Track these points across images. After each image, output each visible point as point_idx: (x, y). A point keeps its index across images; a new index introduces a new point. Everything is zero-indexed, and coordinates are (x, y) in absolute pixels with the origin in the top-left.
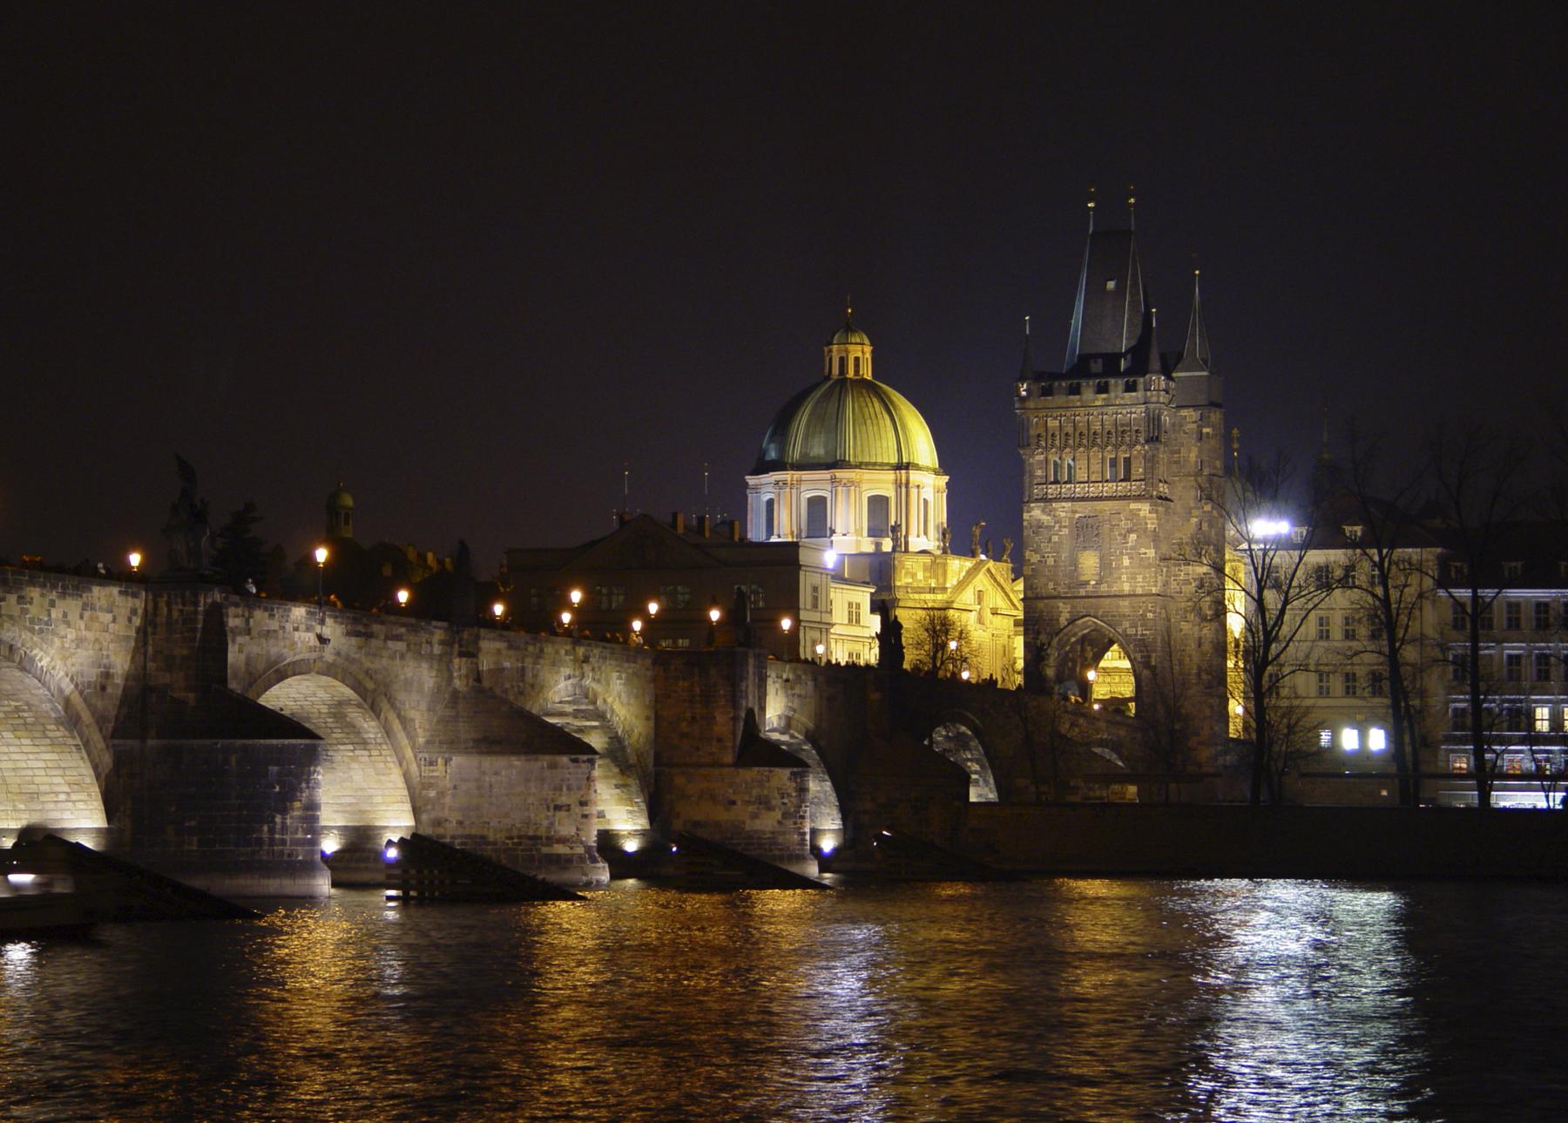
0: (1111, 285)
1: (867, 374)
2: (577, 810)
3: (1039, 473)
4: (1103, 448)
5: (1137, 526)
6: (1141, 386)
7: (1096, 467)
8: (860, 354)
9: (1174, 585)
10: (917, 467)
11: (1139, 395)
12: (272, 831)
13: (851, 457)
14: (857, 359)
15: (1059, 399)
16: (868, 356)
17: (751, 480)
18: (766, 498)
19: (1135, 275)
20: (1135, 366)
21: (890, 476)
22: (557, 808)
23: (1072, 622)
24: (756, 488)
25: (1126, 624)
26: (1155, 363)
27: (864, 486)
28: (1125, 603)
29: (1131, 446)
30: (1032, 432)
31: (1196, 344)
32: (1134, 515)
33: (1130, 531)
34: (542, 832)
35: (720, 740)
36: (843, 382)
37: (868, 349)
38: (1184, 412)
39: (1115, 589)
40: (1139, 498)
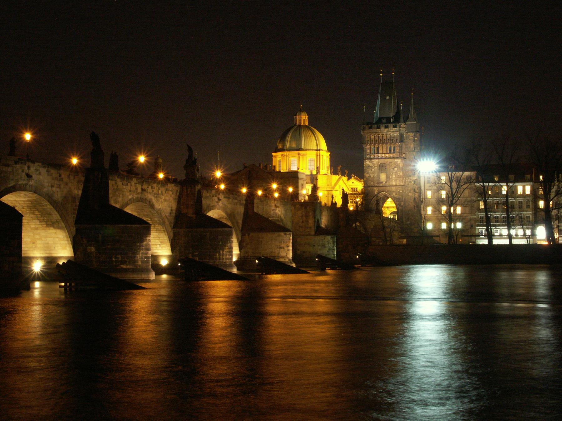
0: (388, 98)
1: (307, 124)
2: (286, 248)
3: (368, 151)
4: (387, 144)
5: (397, 165)
6: (398, 126)
7: (385, 149)
8: (304, 119)
9: (407, 183)
10: (322, 150)
11: (397, 129)
12: (220, 255)
13: (303, 147)
14: (304, 120)
15: (374, 130)
16: (307, 118)
17: (274, 154)
18: (278, 159)
19: (394, 95)
20: (396, 120)
21: (314, 153)
22: (281, 248)
23: (378, 193)
24: (275, 157)
25: (394, 194)
26: (402, 120)
27: (307, 156)
28: (394, 188)
29: (395, 143)
30: (366, 140)
31: (412, 114)
32: (396, 163)
33: (395, 167)
34: (276, 255)
35: (310, 228)
36: (300, 126)
37: (307, 117)
38: (409, 134)
39: (391, 184)
40: (397, 158)
